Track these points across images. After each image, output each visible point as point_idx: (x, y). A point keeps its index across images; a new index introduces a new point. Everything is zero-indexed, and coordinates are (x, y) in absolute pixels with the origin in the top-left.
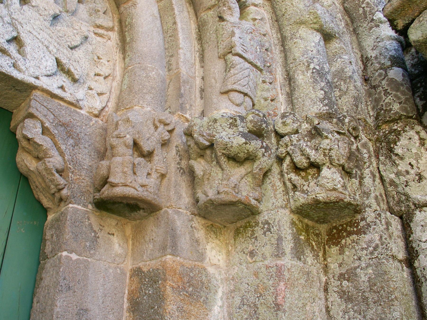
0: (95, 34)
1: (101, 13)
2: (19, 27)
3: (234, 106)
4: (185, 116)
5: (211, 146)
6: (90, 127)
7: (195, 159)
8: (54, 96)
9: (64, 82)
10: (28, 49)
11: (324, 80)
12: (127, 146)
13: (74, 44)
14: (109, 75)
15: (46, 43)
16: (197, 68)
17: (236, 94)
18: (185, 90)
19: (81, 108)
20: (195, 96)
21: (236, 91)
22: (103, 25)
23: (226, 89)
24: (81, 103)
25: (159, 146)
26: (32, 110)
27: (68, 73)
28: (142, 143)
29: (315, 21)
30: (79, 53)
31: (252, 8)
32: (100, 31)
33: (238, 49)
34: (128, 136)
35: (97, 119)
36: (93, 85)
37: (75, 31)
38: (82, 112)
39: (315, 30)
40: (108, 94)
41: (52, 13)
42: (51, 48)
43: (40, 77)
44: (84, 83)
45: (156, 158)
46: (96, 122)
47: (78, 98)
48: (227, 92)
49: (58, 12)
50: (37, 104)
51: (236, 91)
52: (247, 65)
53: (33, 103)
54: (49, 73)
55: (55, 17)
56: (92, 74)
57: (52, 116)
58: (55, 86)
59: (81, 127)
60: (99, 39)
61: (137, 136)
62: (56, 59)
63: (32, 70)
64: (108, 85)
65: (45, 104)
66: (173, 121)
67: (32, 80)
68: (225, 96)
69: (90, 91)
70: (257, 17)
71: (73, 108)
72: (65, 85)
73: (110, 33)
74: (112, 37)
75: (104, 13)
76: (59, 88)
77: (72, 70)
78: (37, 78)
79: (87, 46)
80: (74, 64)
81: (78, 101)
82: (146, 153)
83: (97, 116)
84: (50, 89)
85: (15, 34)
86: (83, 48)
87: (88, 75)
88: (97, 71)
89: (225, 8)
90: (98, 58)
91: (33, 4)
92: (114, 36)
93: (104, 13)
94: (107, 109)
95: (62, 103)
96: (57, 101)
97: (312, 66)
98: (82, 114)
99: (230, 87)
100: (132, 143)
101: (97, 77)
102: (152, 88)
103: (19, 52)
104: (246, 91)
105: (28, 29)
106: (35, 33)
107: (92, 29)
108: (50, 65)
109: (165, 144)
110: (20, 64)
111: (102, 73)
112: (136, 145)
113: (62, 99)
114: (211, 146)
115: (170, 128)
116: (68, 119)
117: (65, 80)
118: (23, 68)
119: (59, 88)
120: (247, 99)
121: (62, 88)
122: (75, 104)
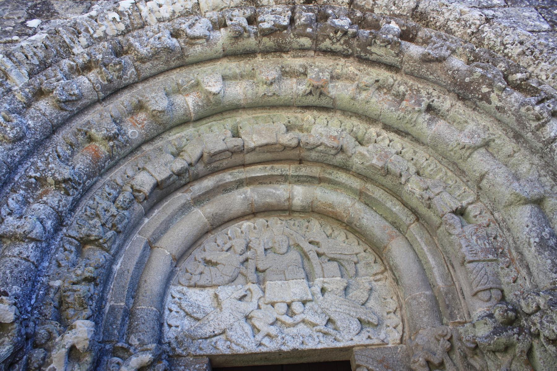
0: (376, 281)
1: (373, 264)
2: (328, 311)
3: (485, 303)
4: (456, 321)
5: (477, 347)
6: (399, 354)
7: (473, 357)
8: (366, 346)
9: (369, 332)
10: (339, 323)
11: (547, 249)
12: (423, 366)
13: (364, 299)
14: (397, 308)
15: (347, 312)
16: (452, 274)
17: (482, 293)
18: (449, 300)
19: (387, 344)
20: (459, 299)
21: (481, 291)
22: (378, 271)
23: (474, 293)
24: (385, 341)
25: (446, 354)
26: (357, 363)
27: (369, 323)
28: (432, 360)
29: (518, 199)
30: (371, 303)
31: (470, 207)
32: (378, 277)
33: (469, 258)
34: (421, 359)
35: (401, 345)
36: (388, 322)
37: (362, 290)
38: (390, 345)
39: (523, 204)
40: (401, 323)
41: (342, 288)
42: (351, 314)
43: (354, 338)
44: (383, 323)
45: (447, 365)
46: (401, 348)
47: (382, 339)
48: (475, 294)
49: (346, 285)
50: (358, 359)
51: (481, 291)
52: (480, 265)
53: (356, 357)
54: (357, 332)
55: (346, 289)
56: (385, 314)
57: (371, 360)
58: (364, 339)
59: (393, 357)
60: (379, 283)
61: (427, 356)
62: (358, 318)
63: (346, 337)
64: (399, 316)
65: (364, 354)
66: (449, 331)
67: (350, 344)
68: (475, 297)
69: (388, 329)
70: (476, 214)
71: (382, 346)
72: (370, 334)
73: (386, 274)
74: (387, 275)
75: (375, 263)
76: (367, 339)
77: (371, 320)
78: (352, 340)
79: (375, 294)
80: (370, 315)
81: (383, 341)
82: (437, 365)
83: (399, 344)
84: (362, 343)
85: (327, 318)
86: (372, 298)
87: (382, 316)
88: (388, 310)
89: (447, 226)
90: (385, 299)
91: (329, 290)
92: (388, 274)
93: (375, 263)
94: (405, 335)
95: (374, 347)
96: (370, 347)
97: (532, 240)
98: (390, 348)
99: (475, 290)
100: (425, 363)
101: (389, 316)
102: (425, 311)
103: (335, 329)
104: (488, 286)
105: (333, 309)
106: (338, 310)
107: (372, 278)
108: (355, 325)
109: (450, 351)
110: (338, 336)
111: (391, 310)
112: (428, 362)
113: (373, 345)
114: (477, 347)
115: (448, 337)
116: (382, 356)
117: (368, 330)
118: (341, 338)
119: (367, 339)
120: (493, 291)
121: (369, 337)
122: (383, 343)
